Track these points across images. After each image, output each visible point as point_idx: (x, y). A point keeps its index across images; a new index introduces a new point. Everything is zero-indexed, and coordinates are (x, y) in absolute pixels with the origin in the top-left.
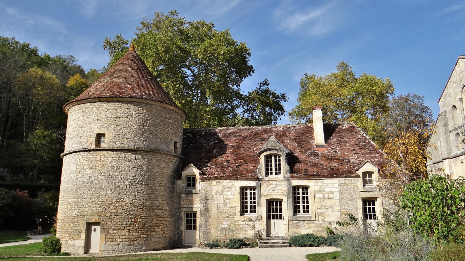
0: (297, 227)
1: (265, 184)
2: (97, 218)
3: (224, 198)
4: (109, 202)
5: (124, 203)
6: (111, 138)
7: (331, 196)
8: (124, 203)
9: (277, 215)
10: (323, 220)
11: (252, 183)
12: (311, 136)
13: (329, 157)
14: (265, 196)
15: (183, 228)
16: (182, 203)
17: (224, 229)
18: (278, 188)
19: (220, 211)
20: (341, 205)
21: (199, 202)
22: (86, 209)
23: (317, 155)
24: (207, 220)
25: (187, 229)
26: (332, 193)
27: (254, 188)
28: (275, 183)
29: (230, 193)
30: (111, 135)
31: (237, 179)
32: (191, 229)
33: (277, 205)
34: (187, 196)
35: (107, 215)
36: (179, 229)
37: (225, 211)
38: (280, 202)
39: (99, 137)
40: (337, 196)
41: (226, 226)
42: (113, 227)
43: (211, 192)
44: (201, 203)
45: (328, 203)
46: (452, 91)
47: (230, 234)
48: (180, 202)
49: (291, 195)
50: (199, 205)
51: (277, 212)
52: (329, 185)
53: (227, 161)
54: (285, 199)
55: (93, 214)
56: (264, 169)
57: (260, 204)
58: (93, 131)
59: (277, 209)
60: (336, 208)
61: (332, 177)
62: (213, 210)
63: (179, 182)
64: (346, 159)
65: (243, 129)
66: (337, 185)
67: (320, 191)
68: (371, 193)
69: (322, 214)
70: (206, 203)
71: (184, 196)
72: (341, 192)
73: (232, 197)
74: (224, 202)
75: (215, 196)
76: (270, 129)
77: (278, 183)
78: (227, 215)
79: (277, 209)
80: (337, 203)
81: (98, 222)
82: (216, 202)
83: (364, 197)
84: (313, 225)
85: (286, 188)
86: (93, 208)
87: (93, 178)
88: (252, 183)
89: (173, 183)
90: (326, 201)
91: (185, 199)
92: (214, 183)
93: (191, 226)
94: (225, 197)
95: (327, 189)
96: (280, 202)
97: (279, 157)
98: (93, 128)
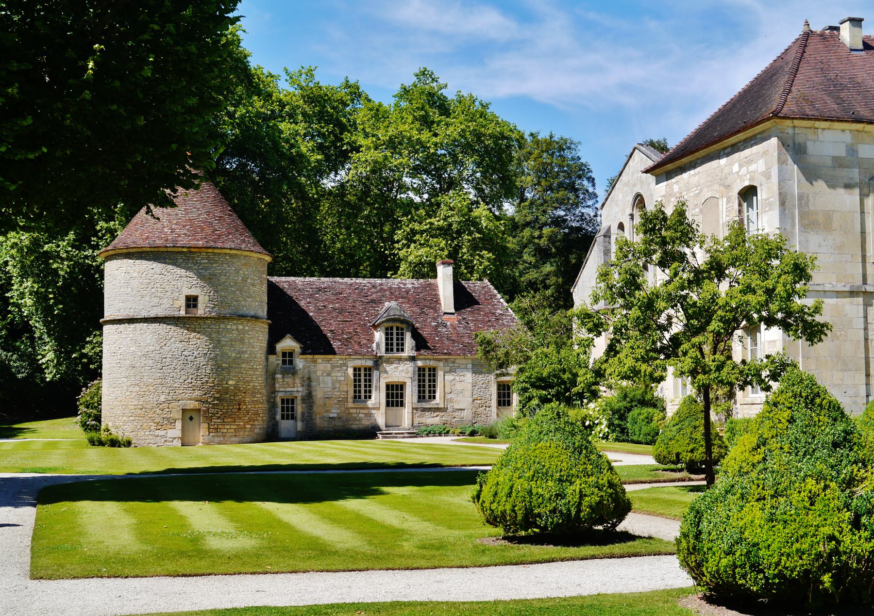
9: (397, 402)
12: (435, 301)
13: (461, 330)
15: (278, 417)
16: (277, 385)
20: (473, 390)
21: (299, 385)
25: (283, 418)
29: (340, 374)
32: (288, 419)
33: (397, 390)
34: (283, 378)
36: (275, 418)
38: (401, 387)
39: (192, 302)
41: (335, 415)
43: (316, 372)
44: (303, 386)
46: (620, 197)
48: (274, 384)
49: (417, 377)
50: (300, 389)
51: (397, 397)
55: (190, 399)
56: (384, 345)
57: (378, 388)
59: (397, 394)
60: (468, 393)
62: (319, 394)
63: (272, 358)
65: (342, 283)
70: (309, 386)
71: (279, 376)
73: (343, 378)
74: (333, 384)
75: (321, 378)
76: (381, 284)
79: (397, 394)
80: (470, 387)
82: (322, 385)
89: (267, 359)
93: (288, 415)
94: (334, 378)
96: (401, 387)
97: (402, 329)
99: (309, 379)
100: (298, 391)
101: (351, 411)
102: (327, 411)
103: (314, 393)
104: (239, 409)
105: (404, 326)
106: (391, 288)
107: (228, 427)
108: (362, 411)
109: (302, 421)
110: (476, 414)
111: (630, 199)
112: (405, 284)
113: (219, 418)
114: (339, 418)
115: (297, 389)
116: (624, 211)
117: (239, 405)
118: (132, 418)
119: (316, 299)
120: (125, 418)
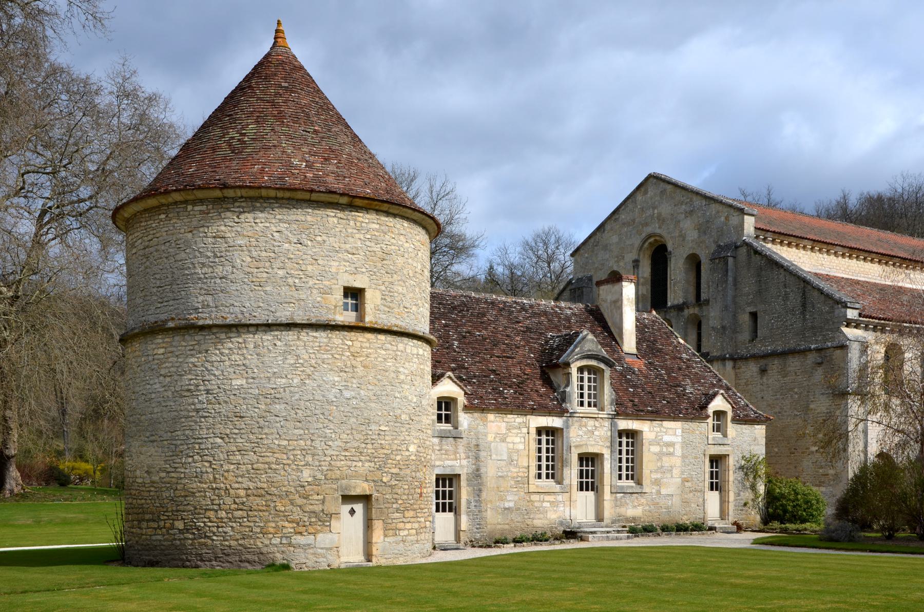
0: (621, 506)
1: (576, 425)
2: (365, 485)
3: (508, 449)
4: (385, 451)
5: (407, 453)
6: (379, 302)
7: (671, 450)
8: (407, 453)
10: (659, 492)
11: (555, 422)
14: (576, 447)
17: (508, 509)
18: (596, 433)
19: (500, 474)
21: (463, 455)
22: (339, 464)
23: (634, 373)
24: (478, 492)
25: (437, 510)
26: (672, 444)
27: (551, 432)
28: (591, 423)
29: (517, 440)
30: (378, 294)
31: (533, 411)
32: (444, 510)
34: (440, 444)
35: (385, 480)
37: (509, 474)
40: (678, 452)
41: (511, 504)
42: (394, 506)
45: (667, 462)
46: (615, 239)
47: (519, 519)
50: (464, 462)
52: (671, 432)
53: (494, 371)
54: (607, 453)
57: (564, 463)
58: (334, 277)
60: (676, 472)
61: (675, 418)
62: (490, 471)
64: (679, 386)
66: (680, 431)
67: (657, 442)
68: (721, 448)
69: (657, 482)
70: (477, 458)
72: (685, 444)
73: (521, 447)
76: (531, 306)
77: (597, 424)
78: (513, 483)
80: (677, 461)
81: (368, 493)
82: (494, 457)
83: (712, 453)
84: (643, 500)
85: (609, 433)
86: (354, 463)
87: (347, 394)
88: (555, 422)
90: (664, 459)
91: (438, 448)
92: (491, 417)
93: (444, 504)
94: (511, 446)
95: (667, 438)
98: (333, 270)
99: (478, 445)
100: (461, 466)
101: (535, 497)
102: (502, 499)
103: (483, 470)
104: (421, 495)
105: (602, 366)
106: (545, 313)
107: (408, 526)
108: (547, 498)
109: (468, 514)
110: (686, 502)
111: (637, 242)
112: (560, 308)
113: (397, 510)
114: (518, 509)
115: (460, 465)
116: (620, 257)
117: (421, 488)
118: (239, 514)
119: (454, 320)
120: (223, 514)
